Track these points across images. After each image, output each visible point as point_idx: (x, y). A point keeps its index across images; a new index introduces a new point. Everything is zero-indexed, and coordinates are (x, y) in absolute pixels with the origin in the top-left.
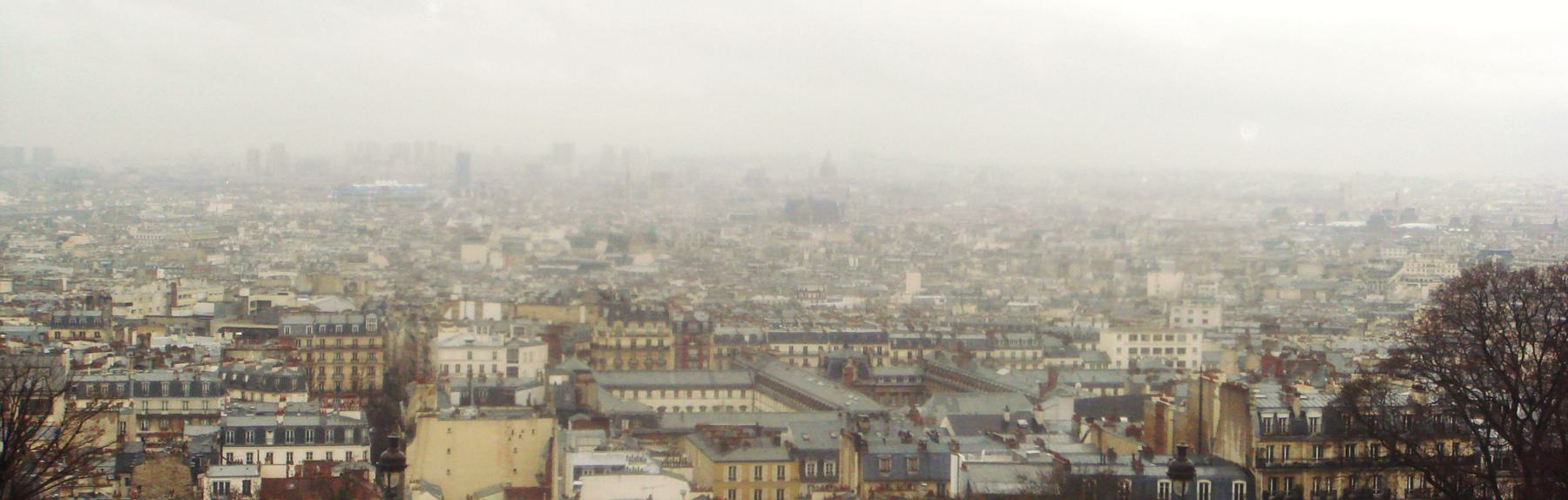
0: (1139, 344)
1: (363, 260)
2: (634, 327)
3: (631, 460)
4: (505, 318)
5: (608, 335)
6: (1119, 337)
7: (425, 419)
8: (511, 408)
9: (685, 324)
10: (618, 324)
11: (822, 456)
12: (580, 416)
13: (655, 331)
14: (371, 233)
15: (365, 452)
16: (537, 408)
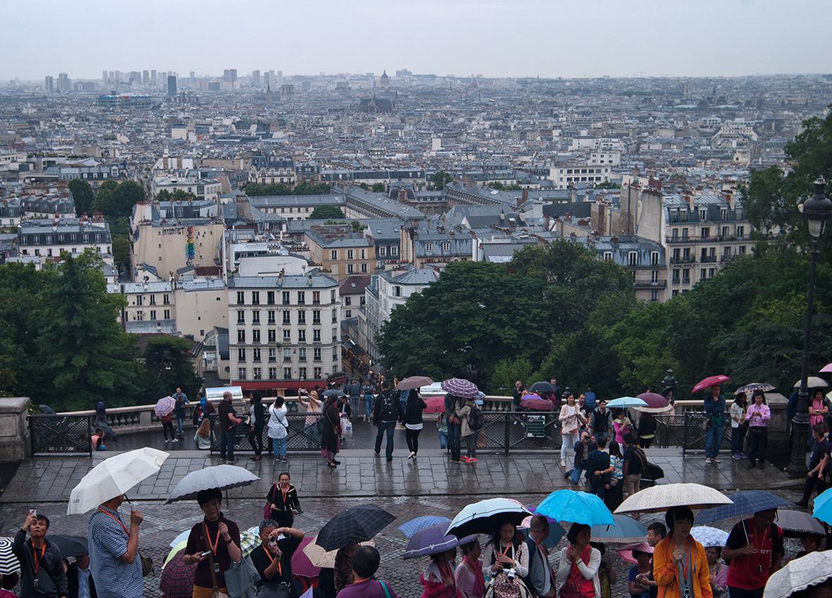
0: (573, 176)
1: (114, 139)
2: (272, 171)
3: (270, 248)
4: (195, 168)
5: (257, 177)
6: (561, 171)
7: (144, 226)
8: (197, 219)
9: (303, 168)
10: (263, 169)
11: (390, 243)
12: (238, 223)
13: (285, 173)
14: (119, 123)
15: (108, 248)
16: (213, 218)
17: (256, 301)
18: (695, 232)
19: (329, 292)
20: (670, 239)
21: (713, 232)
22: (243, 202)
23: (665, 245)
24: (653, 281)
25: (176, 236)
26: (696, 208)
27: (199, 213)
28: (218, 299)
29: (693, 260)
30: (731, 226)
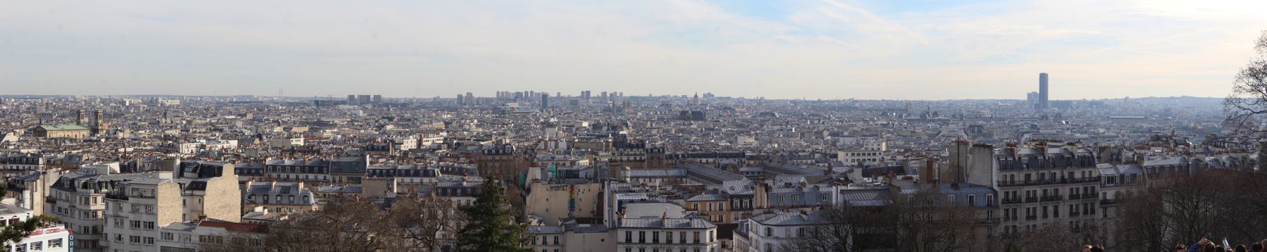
6: (847, 154)
9: (652, 150)
10: (621, 150)
13: (638, 153)
17: (642, 240)
18: (1020, 176)
19: (708, 232)
20: (1001, 184)
21: (1034, 177)
22: (615, 166)
23: (996, 188)
24: (988, 219)
25: (560, 192)
26: (1019, 158)
27: (578, 174)
28: (603, 240)
29: (1020, 201)
30: (1046, 172)
